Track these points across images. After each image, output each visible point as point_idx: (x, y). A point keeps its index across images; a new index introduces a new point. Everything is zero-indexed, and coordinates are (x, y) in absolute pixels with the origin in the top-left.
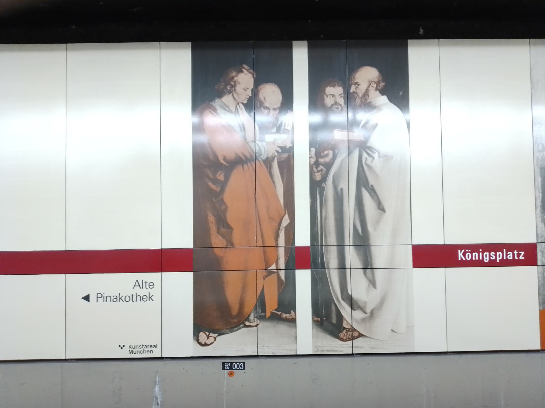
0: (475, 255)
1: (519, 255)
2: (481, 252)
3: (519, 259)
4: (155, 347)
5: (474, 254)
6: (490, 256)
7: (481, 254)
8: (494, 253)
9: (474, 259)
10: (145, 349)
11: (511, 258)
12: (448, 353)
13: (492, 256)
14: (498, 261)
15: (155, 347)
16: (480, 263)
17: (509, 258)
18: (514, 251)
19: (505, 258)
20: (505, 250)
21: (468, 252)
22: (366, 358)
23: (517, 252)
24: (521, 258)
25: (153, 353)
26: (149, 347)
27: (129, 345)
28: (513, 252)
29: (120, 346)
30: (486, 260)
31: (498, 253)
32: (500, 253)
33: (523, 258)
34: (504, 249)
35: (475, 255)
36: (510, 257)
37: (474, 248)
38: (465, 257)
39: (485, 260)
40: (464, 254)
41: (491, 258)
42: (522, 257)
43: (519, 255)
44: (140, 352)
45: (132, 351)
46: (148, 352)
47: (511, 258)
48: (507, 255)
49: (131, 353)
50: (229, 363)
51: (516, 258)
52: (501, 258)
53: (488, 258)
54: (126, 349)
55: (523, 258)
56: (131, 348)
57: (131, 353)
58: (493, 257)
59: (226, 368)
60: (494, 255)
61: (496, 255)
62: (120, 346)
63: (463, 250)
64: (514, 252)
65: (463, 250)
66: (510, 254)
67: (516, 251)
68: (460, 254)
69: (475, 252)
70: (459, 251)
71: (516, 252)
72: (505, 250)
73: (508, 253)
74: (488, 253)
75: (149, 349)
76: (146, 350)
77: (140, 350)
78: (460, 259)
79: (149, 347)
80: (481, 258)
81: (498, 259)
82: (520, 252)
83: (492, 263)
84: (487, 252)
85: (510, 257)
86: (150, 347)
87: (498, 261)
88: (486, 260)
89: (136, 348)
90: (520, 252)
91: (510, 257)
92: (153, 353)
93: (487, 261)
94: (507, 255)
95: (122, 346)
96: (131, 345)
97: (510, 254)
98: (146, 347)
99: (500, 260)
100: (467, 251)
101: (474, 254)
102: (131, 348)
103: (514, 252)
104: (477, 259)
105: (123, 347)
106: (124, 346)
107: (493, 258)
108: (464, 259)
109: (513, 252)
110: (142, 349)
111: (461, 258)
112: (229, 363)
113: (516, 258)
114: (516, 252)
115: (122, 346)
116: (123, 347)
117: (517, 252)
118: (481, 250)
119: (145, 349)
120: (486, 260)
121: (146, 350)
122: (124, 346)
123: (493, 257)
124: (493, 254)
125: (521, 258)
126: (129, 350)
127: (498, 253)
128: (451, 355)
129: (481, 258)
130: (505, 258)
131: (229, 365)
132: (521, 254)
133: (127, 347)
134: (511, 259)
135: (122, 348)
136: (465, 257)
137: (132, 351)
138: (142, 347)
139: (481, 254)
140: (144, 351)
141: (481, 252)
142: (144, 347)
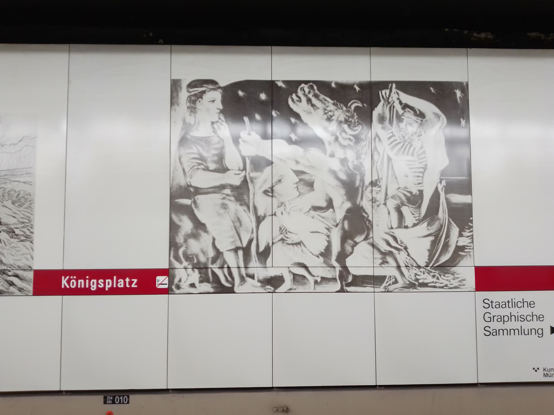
0: (81, 282)
1: (131, 283)
2: (87, 279)
3: (131, 288)
5: (79, 281)
6: (98, 284)
7: (87, 281)
8: (102, 281)
9: (79, 287)
11: (122, 286)
12: (378, 387)
13: (99, 284)
14: (107, 289)
16: (86, 292)
17: (119, 286)
18: (126, 279)
19: (115, 286)
20: (115, 277)
21: (73, 279)
22: (342, 392)
23: (129, 280)
24: (133, 286)
28: (124, 279)
29: (534, 369)
30: (93, 288)
31: (107, 281)
32: (110, 281)
33: (136, 286)
34: (115, 276)
35: (81, 282)
36: (121, 285)
37: (81, 274)
38: (69, 284)
39: (92, 289)
40: (68, 282)
41: (99, 286)
42: (135, 285)
43: (131, 283)
45: (547, 374)
47: (122, 286)
48: (117, 283)
50: (112, 397)
51: (128, 286)
52: (110, 286)
53: (95, 286)
55: (136, 286)
58: (101, 285)
59: (108, 402)
60: (102, 283)
61: (104, 283)
62: (534, 369)
63: (68, 277)
64: (126, 280)
65: (68, 277)
66: (121, 282)
67: (127, 278)
68: (64, 282)
69: (80, 279)
70: (63, 277)
71: (127, 280)
72: (115, 277)
73: (119, 281)
74: (95, 281)
78: (63, 287)
80: (87, 286)
81: (107, 287)
82: (133, 280)
83: (100, 292)
84: (94, 279)
85: (121, 285)
87: (107, 289)
88: (94, 288)
89: (551, 371)
90: (133, 280)
91: (121, 284)
93: (94, 289)
94: (117, 283)
95: (536, 369)
96: (546, 368)
97: (121, 282)
99: (109, 288)
100: (72, 277)
101: (79, 281)
103: (126, 280)
104: (83, 287)
105: (538, 370)
106: (538, 369)
107: (101, 286)
108: (68, 287)
109: (124, 279)
111: (65, 286)
112: (112, 397)
113: (128, 286)
114: (127, 280)
115: (536, 369)
116: (538, 370)
117: (129, 280)
118: (87, 277)
120: (94, 288)
122: (538, 369)
123: (101, 285)
124: (101, 281)
125: (133, 286)
126: (544, 374)
127: (107, 281)
128: (290, 391)
129: (87, 286)
130: (115, 286)
131: (112, 399)
132: (133, 281)
133: (541, 370)
134: (121, 288)
135: (536, 371)
136: (69, 284)
139: (87, 281)
141: (87, 279)
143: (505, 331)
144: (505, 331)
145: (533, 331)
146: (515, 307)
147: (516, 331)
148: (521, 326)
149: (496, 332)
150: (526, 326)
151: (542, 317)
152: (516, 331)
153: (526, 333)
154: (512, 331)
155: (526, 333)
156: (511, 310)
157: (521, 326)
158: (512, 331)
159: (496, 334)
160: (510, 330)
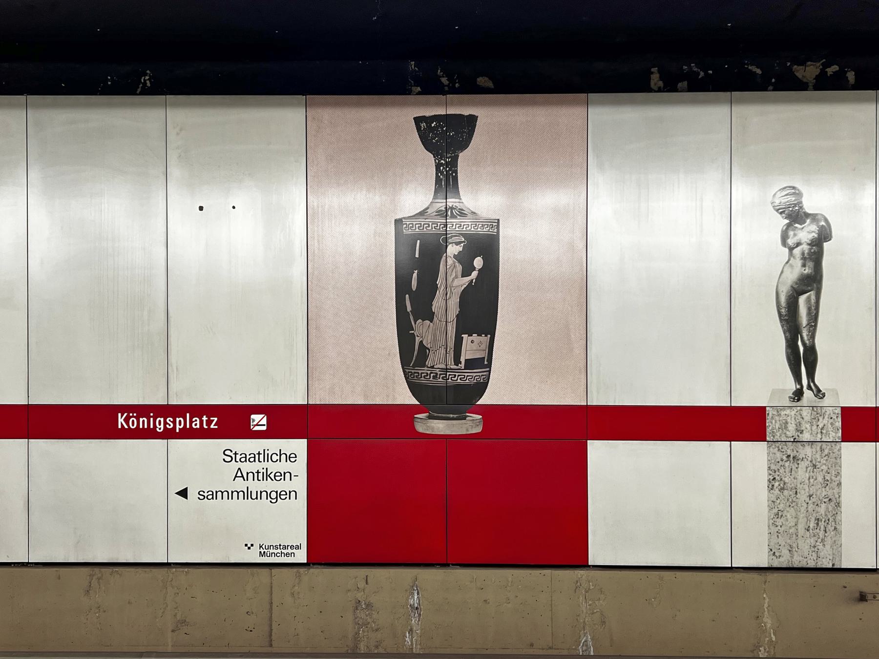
4: (298, 547)
10: (283, 551)
15: (298, 547)
25: (294, 556)
26: (289, 547)
27: (260, 545)
44: (276, 555)
46: (287, 555)
49: (262, 556)
54: (256, 550)
56: (263, 549)
57: (262, 556)
75: (290, 551)
76: (285, 551)
77: (276, 551)
79: (289, 547)
86: (291, 547)
92: (294, 556)
98: (285, 547)
102: (263, 549)
110: (279, 551)
119: (283, 551)
121: (285, 551)
137: (264, 552)
138: (279, 547)
140: (282, 553)
142: (281, 547)
143: (225, 494)
144: (225, 494)
145: (264, 494)
146: (268, 461)
147: (241, 494)
148: (248, 487)
149: (213, 495)
150: (255, 486)
151: (280, 475)
152: (241, 494)
153: (254, 497)
154: (235, 494)
155: (254, 496)
156: (265, 465)
157: (248, 487)
158: (235, 494)
159: (213, 498)
160: (232, 492)
